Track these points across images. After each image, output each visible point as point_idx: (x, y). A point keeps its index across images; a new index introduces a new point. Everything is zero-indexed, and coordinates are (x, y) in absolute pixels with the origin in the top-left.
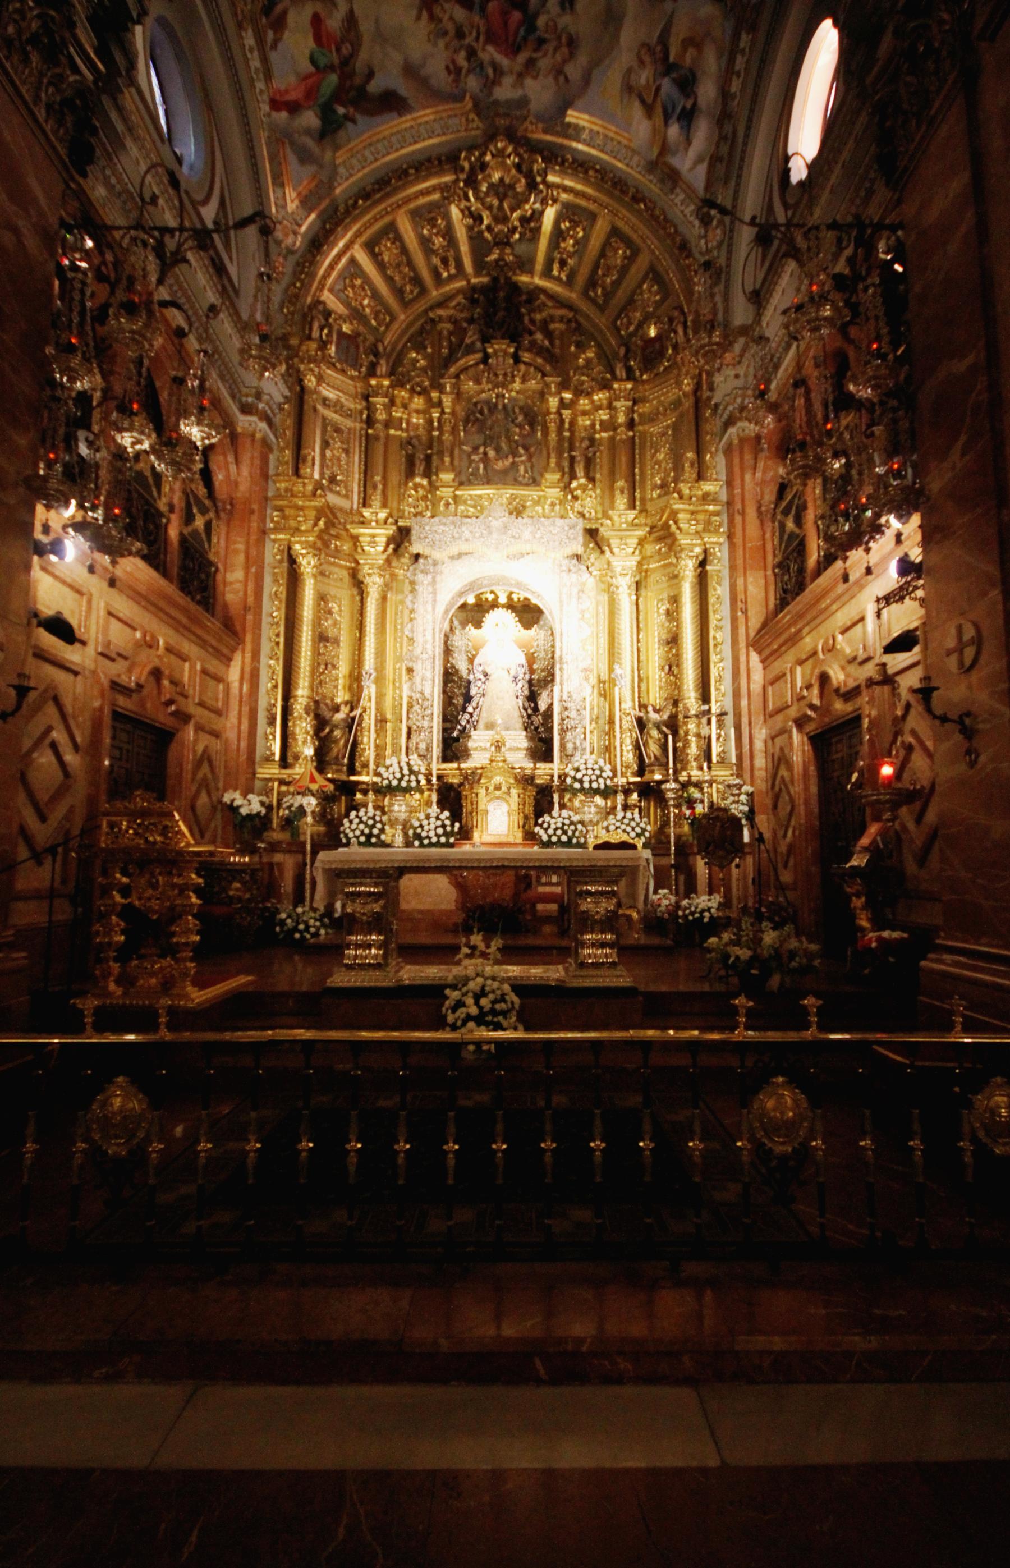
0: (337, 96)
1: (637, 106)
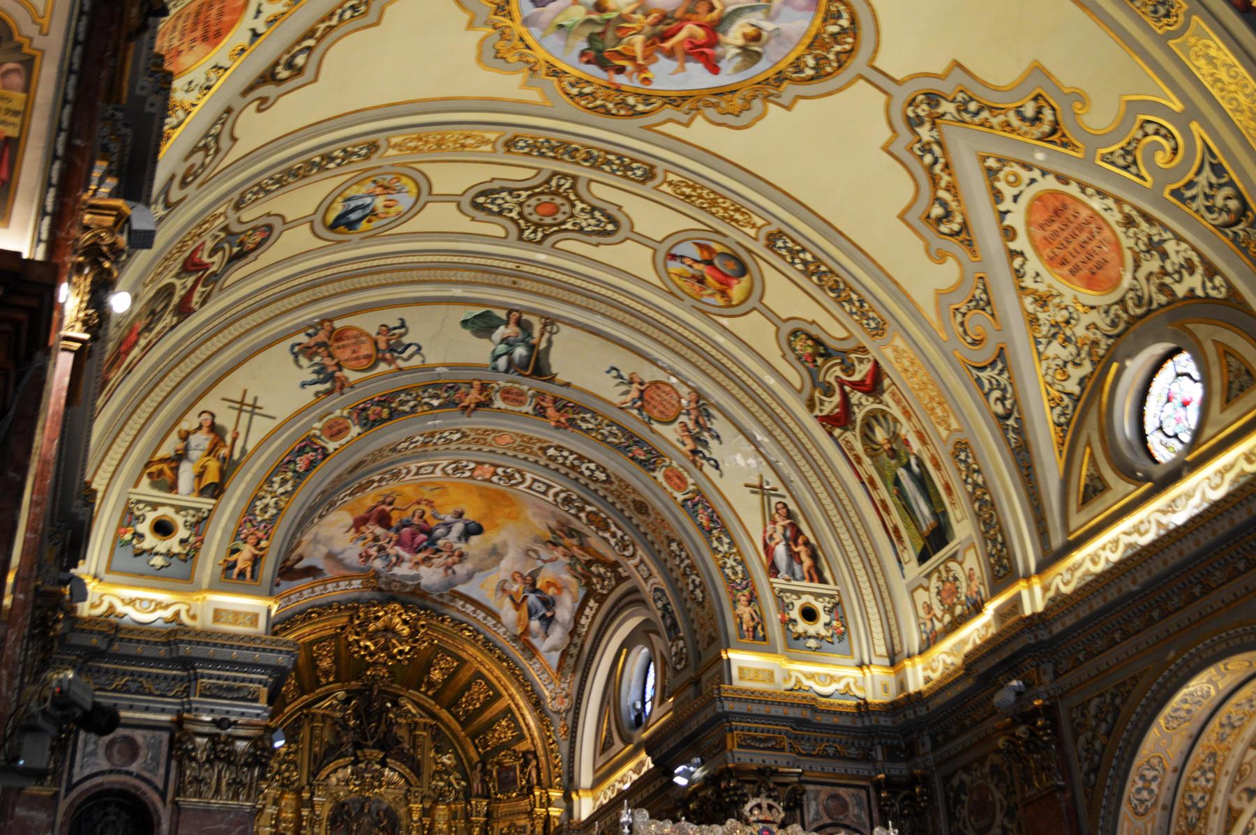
1: (507, 601)
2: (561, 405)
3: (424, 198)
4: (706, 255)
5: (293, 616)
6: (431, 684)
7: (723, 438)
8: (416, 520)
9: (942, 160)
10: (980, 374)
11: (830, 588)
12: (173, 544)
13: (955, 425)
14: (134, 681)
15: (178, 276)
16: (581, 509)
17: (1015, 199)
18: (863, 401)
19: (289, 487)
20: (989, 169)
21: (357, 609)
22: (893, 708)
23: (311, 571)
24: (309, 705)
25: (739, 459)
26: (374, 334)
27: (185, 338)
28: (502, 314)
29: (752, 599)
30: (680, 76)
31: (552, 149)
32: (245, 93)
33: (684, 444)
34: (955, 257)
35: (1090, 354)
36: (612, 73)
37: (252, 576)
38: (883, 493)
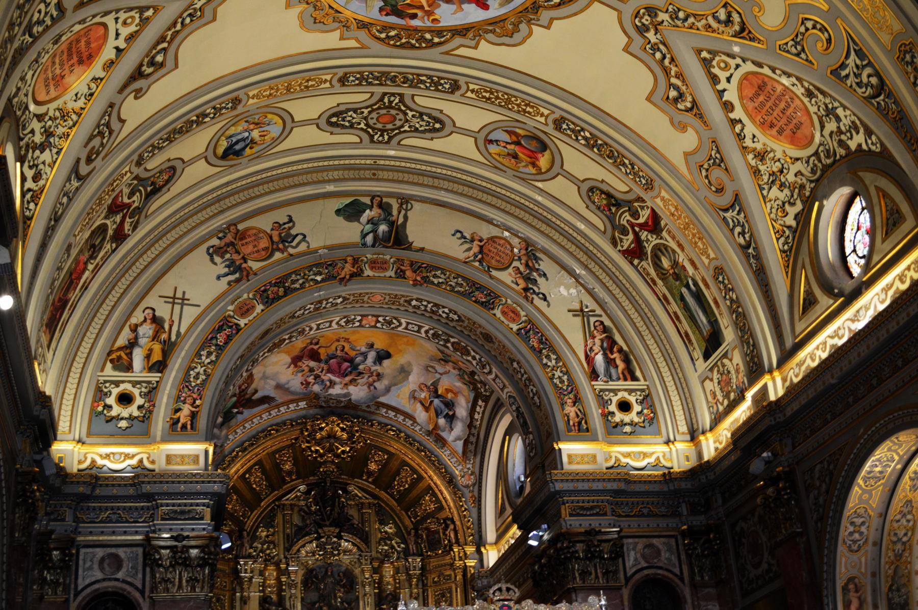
0: (235, 406)
1: (419, 405)
2: (416, 267)
3: (289, 124)
4: (514, 139)
5: (257, 434)
6: (370, 474)
7: (548, 275)
8: (339, 353)
9: (668, 56)
10: (725, 215)
11: (641, 384)
12: (133, 410)
13: (712, 255)
14: (114, 513)
15: (106, 218)
16: (447, 341)
17: (728, 80)
18: (649, 237)
19: (213, 358)
20: (704, 59)
21: (306, 423)
22: (691, 474)
23: (266, 400)
24: (279, 498)
25: (563, 290)
26: (269, 231)
27: (125, 257)
28: (367, 200)
29: (577, 400)
30: (459, 15)
31: (377, 78)
32: (121, 91)
33: (518, 285)
34: (692, 127)
35: (799, 194)
36: (408, 19)
37: (192, 428)
38: (674, 307)
